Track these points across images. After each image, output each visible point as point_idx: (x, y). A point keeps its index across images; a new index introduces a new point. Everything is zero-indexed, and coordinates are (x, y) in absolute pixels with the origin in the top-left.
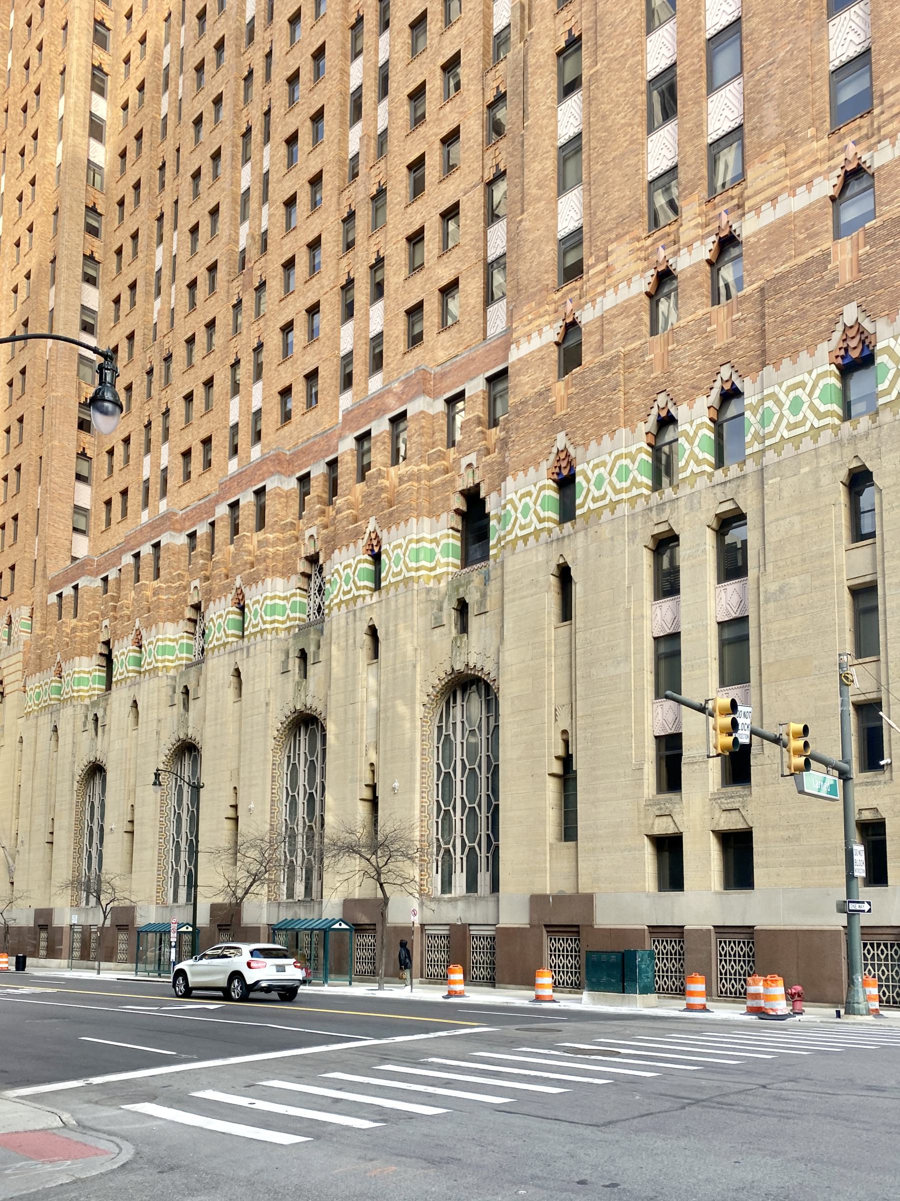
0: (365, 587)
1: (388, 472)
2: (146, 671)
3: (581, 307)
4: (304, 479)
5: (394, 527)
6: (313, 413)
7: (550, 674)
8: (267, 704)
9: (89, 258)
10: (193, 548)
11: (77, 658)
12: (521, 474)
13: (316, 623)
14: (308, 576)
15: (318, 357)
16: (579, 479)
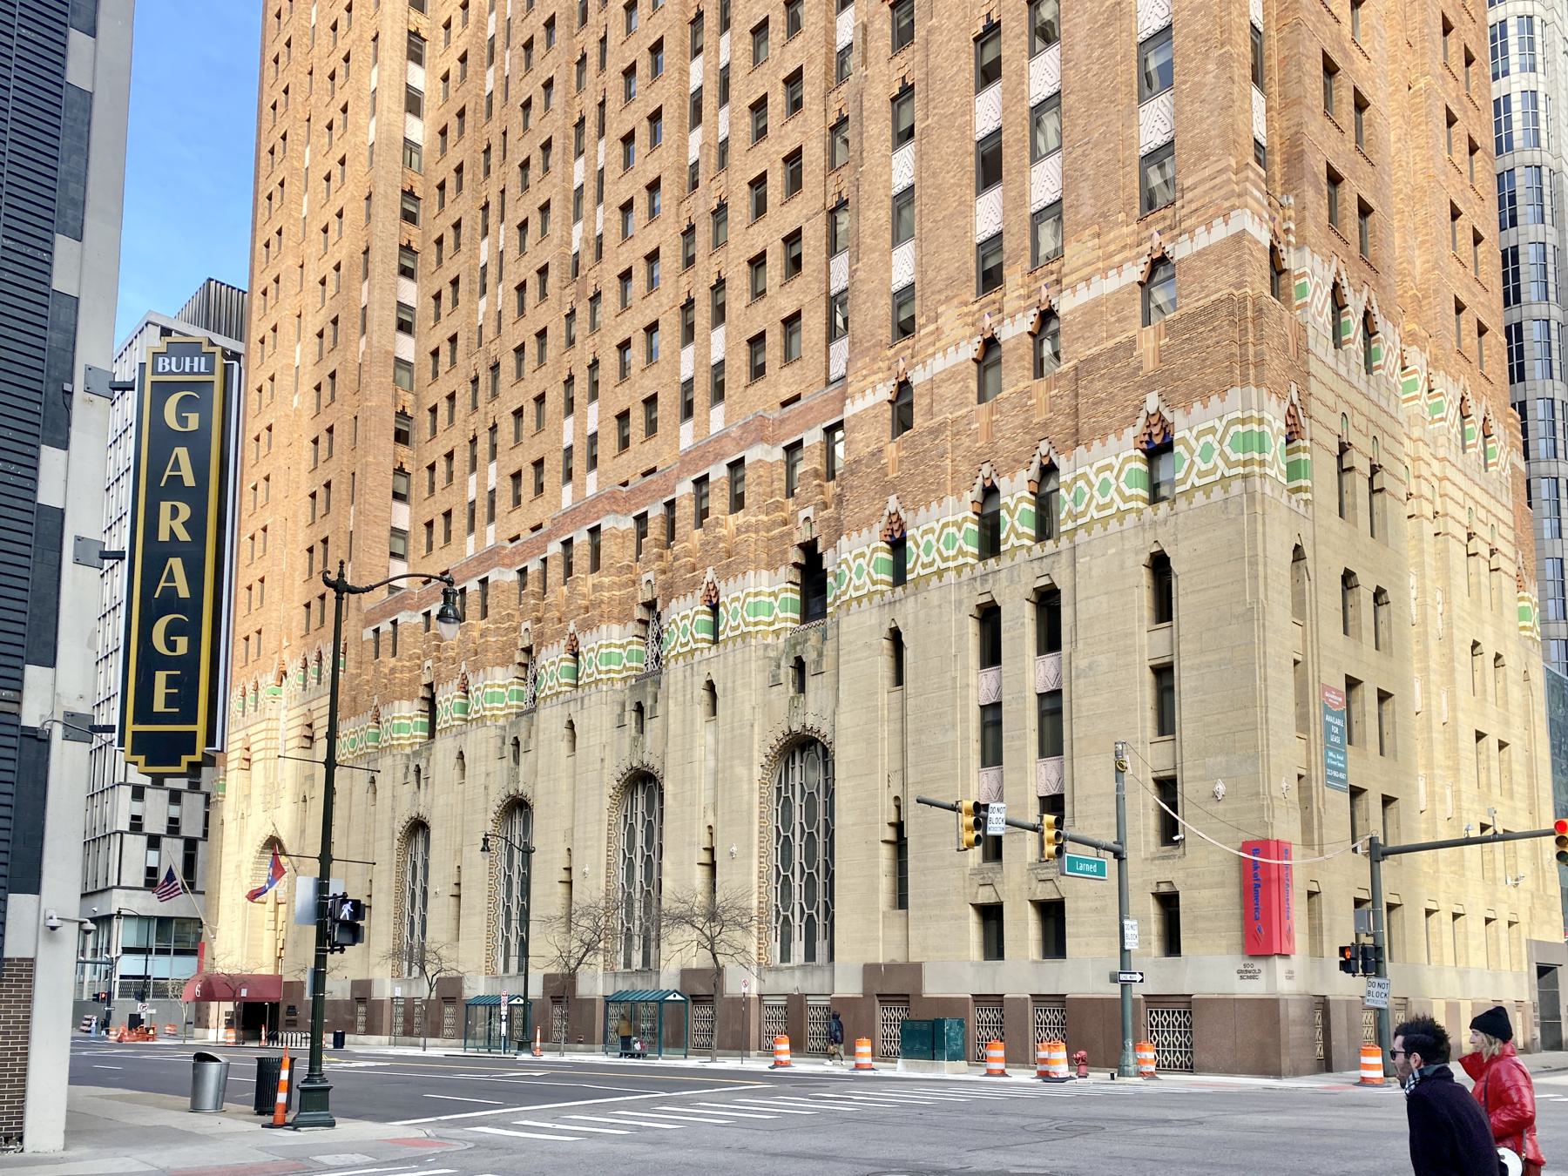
0: (704, 640)
4: (642, 519)
6: (653, 442)
9: (406, 249)
10: (523, 585)
16: (909, 544)
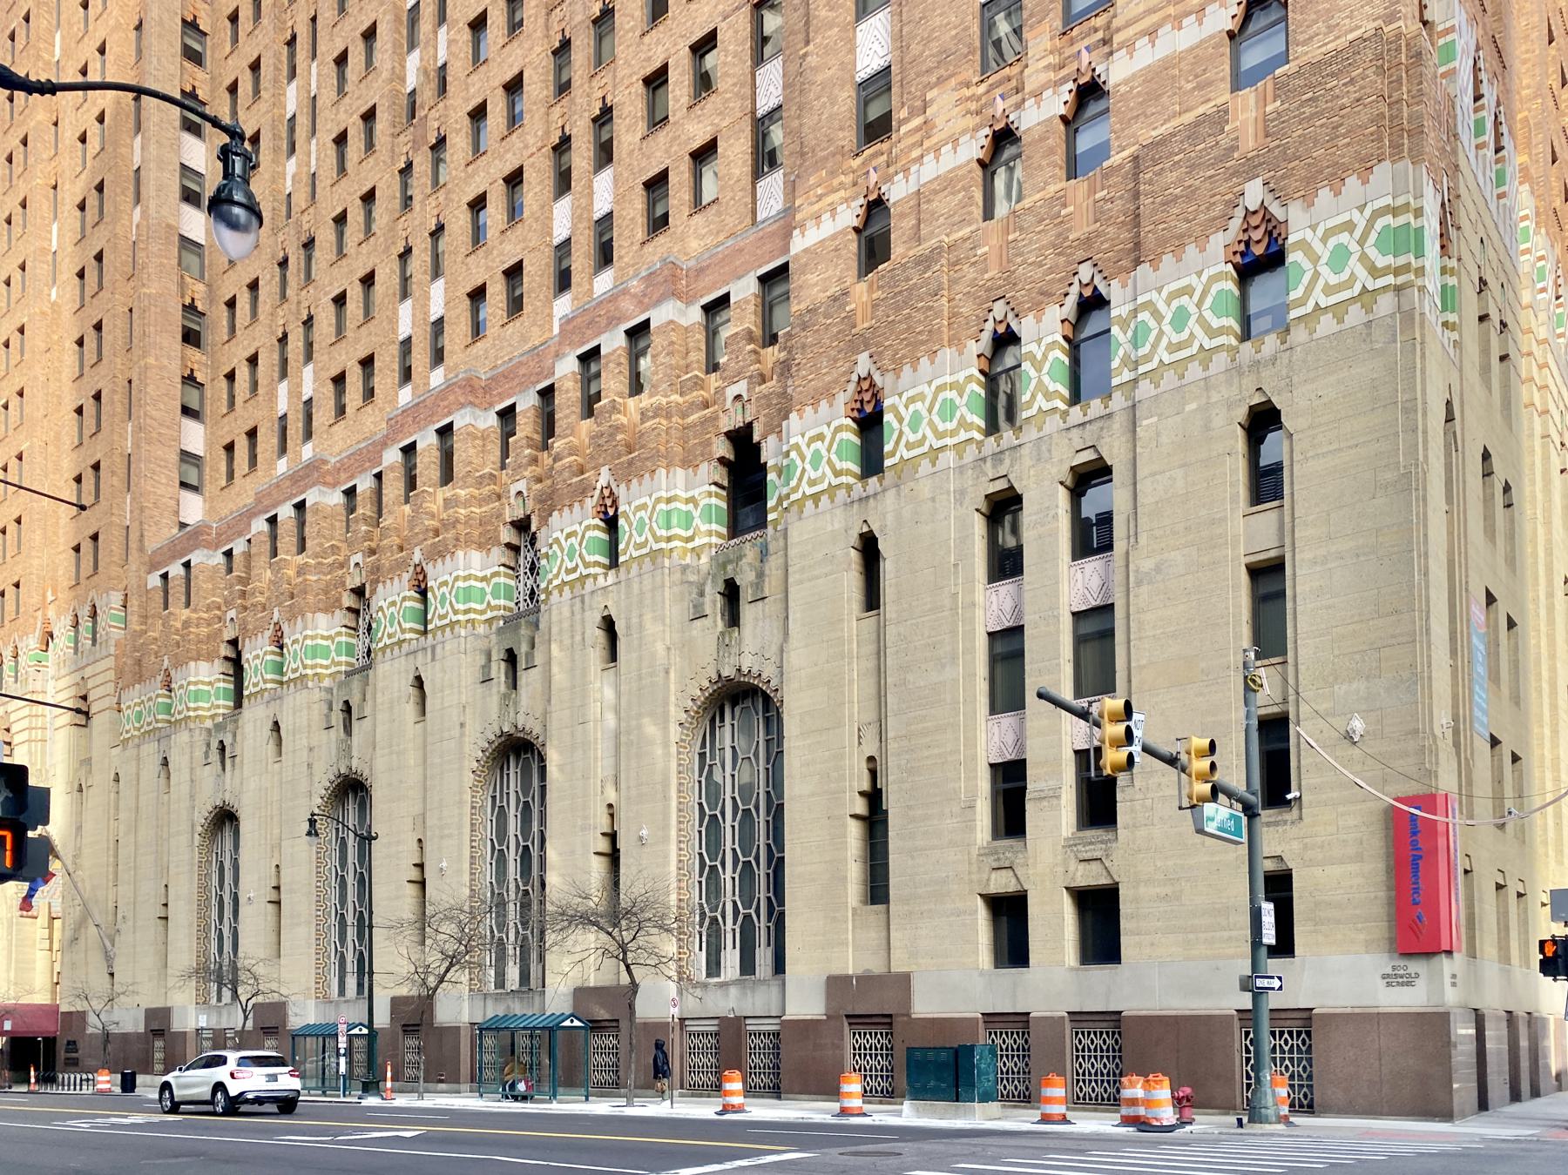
0: (597, 564)
1: (625, 405)
2: (290, 680)
3: (889, 179)
4: (508, 414)
5: (635, 481)
7: (851, 681)
8: (462, 725)
10: (351, 509)
11: (192, 664)
12: (809, 409)
13: (528, 613)
14: (514, 549)
15: (522, 245)
